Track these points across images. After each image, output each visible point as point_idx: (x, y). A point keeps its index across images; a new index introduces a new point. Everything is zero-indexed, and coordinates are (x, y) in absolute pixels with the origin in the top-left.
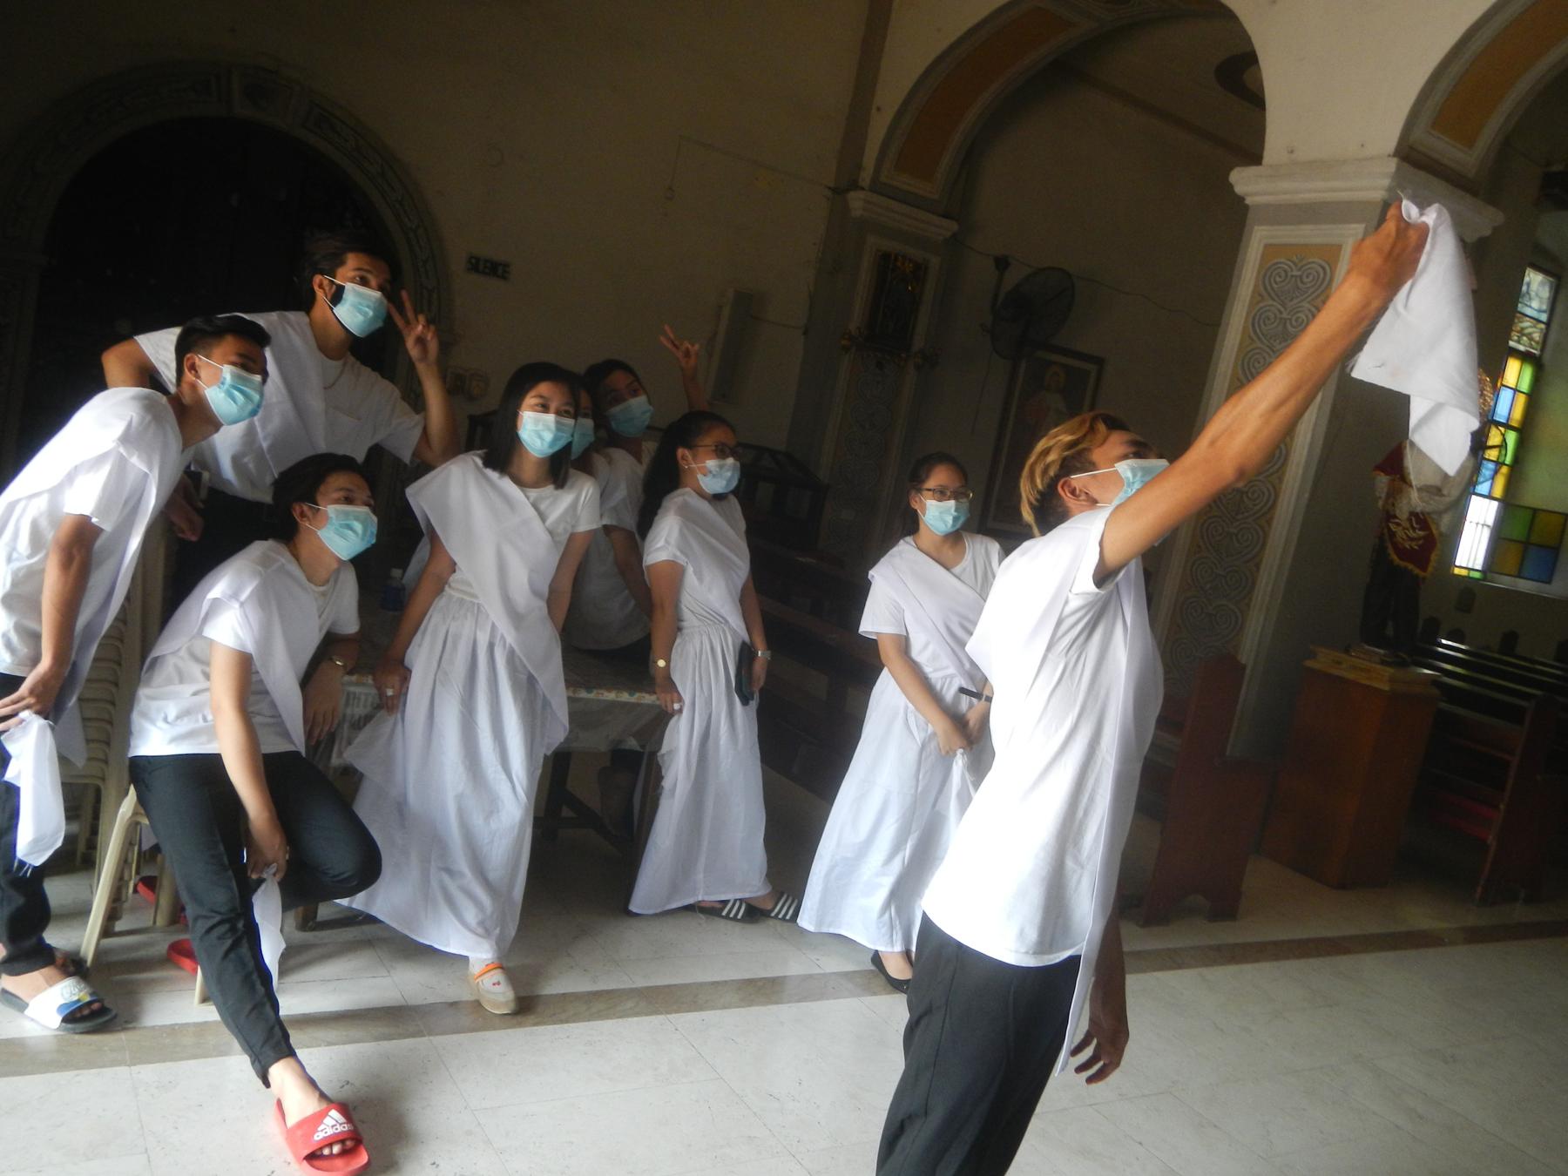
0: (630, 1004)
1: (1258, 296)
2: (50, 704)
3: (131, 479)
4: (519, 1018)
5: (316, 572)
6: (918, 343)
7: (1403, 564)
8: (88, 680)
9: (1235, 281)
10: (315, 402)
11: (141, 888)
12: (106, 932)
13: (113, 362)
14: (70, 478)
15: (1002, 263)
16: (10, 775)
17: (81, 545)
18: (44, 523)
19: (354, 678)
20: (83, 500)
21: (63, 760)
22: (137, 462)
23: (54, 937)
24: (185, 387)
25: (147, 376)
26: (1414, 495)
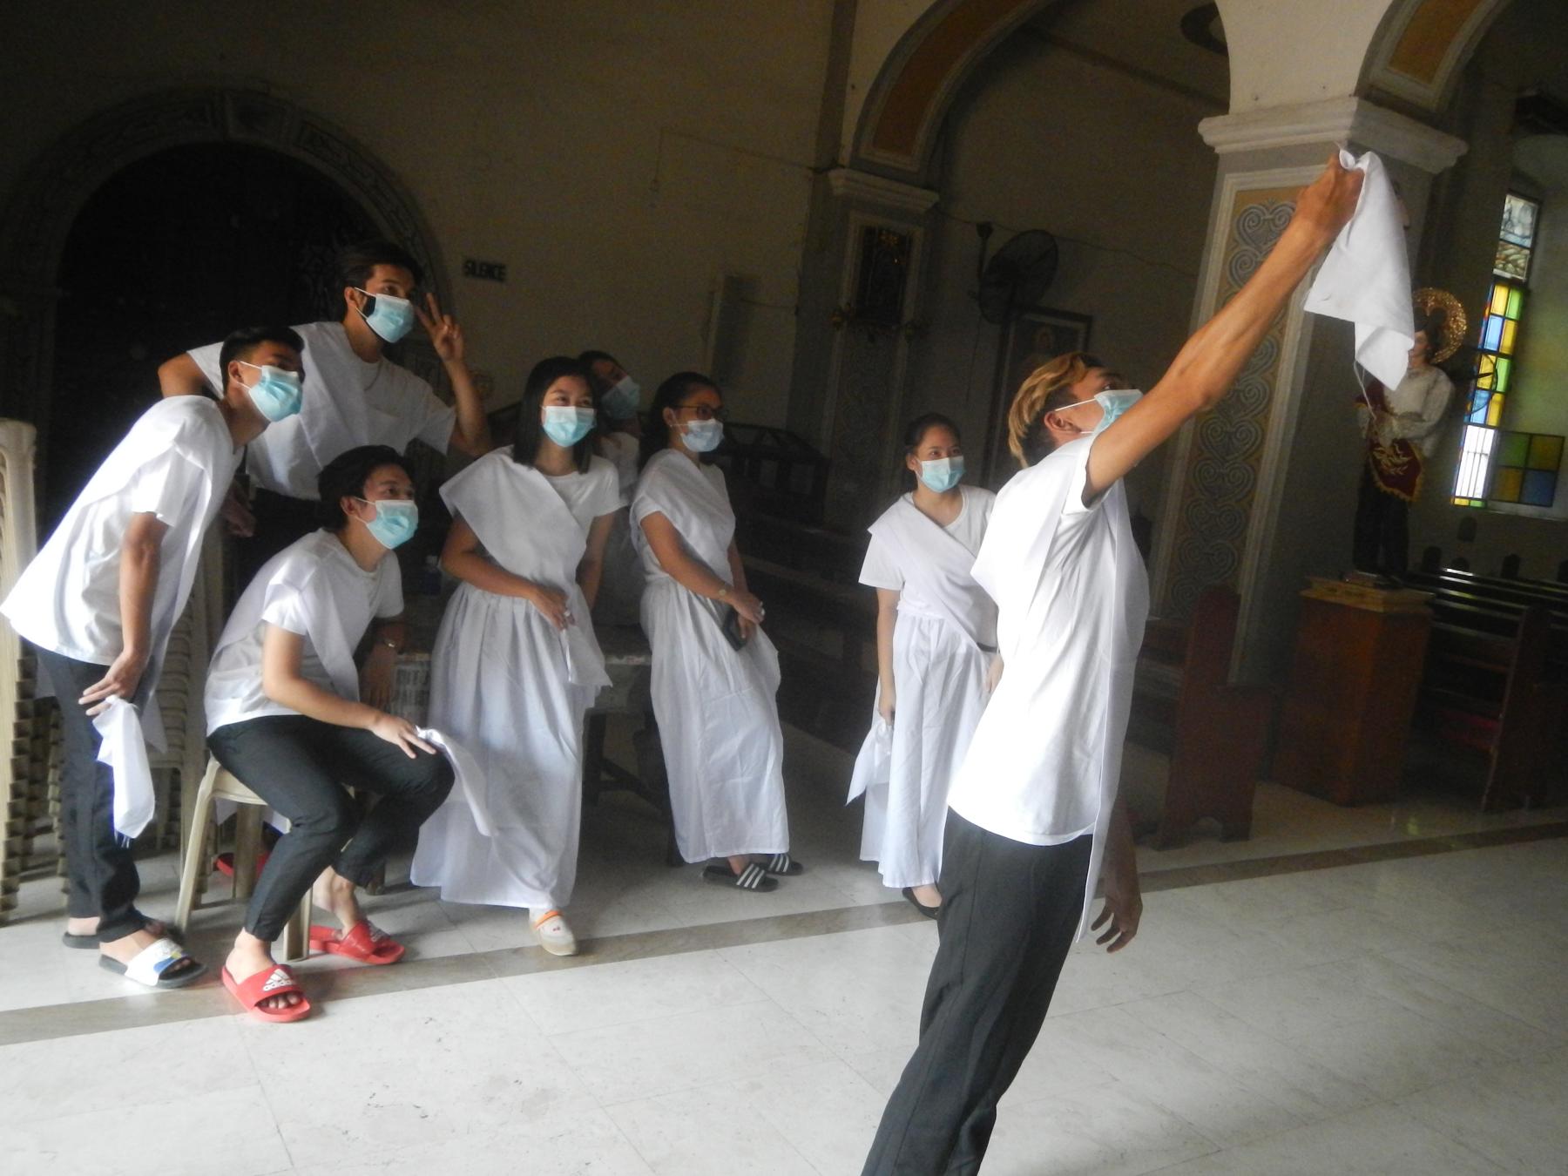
0: (680, 942)
1: (1232, 242)
2: (134, 689)
3: (189, 478)
4: (579, 958)
6: (908, 314)
7: (1389, 490)
9: (1209, 230)
11: (221, 865)
12: (196, 904)
14: (135, 480)
15: (985, 230)
16: (102, 756)
17: (150, 541)
18: (115, 524)
19: (403, 657)
20: (149, 499)
22: (193, 460)
23: (147, 909)
24: (231, 393)
26: (1395, 423)
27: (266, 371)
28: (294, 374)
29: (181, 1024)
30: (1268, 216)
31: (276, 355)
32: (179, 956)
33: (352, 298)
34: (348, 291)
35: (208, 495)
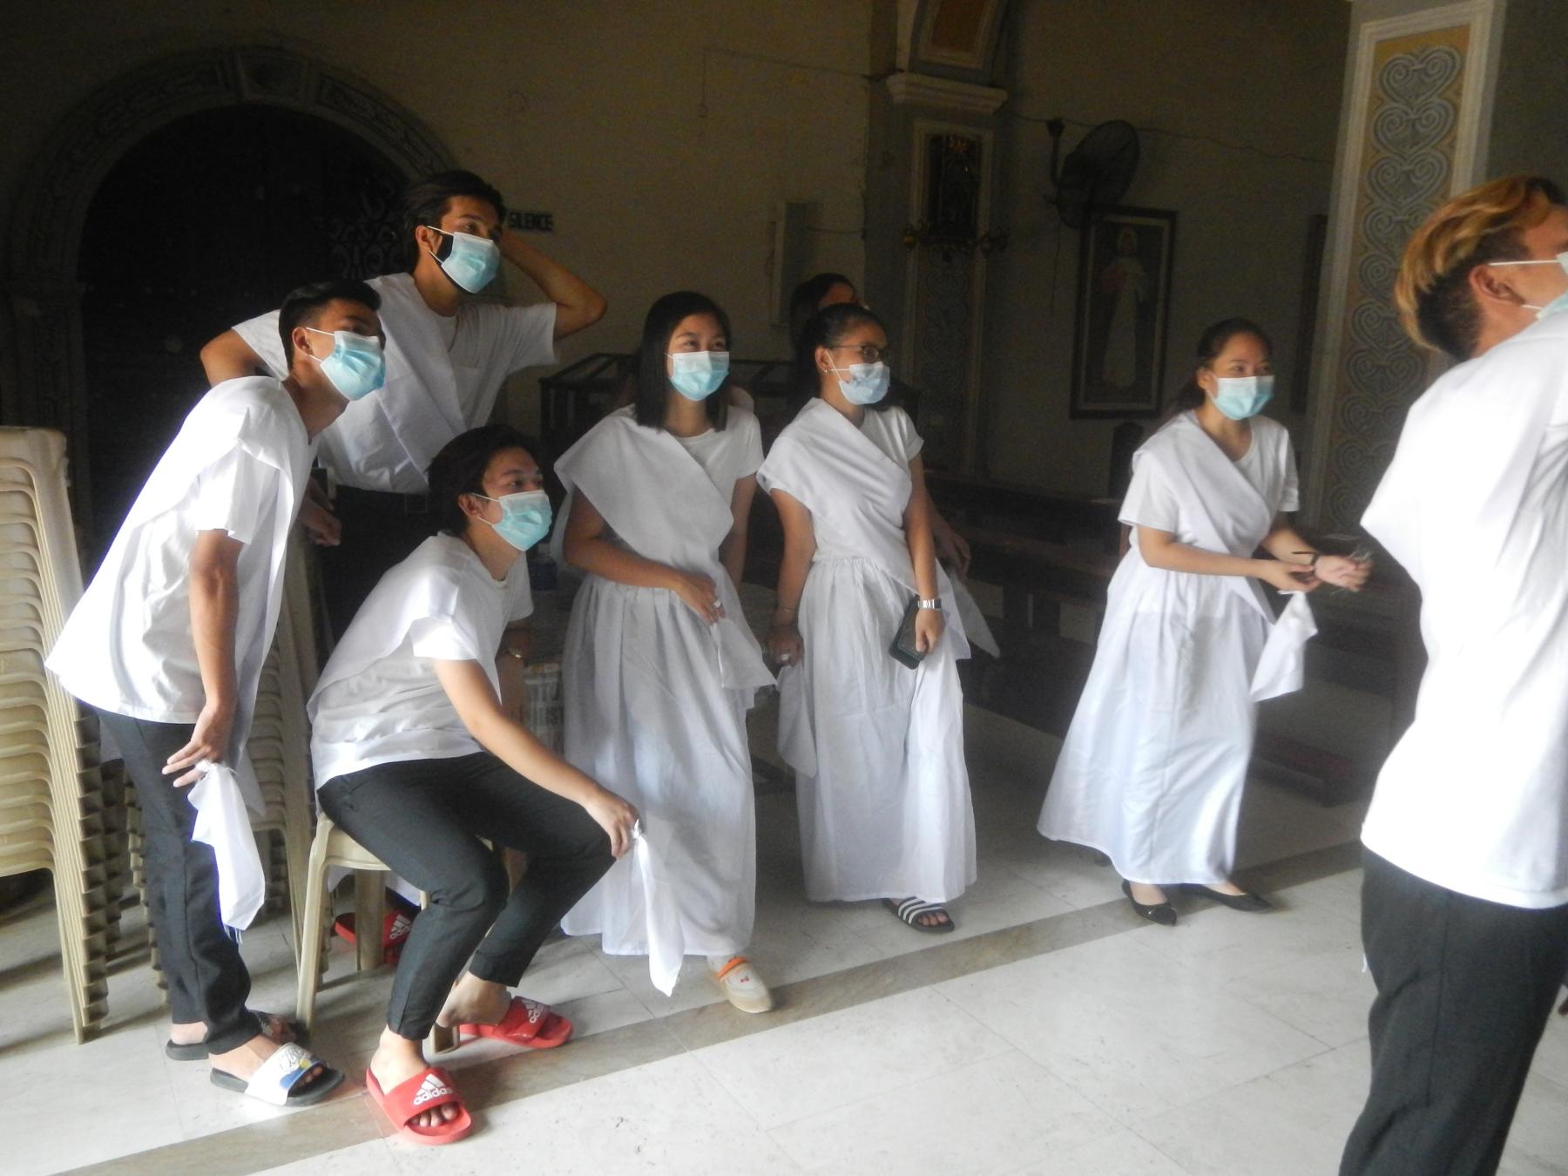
0: (889, 980)
2: (222, 747)
3: (261, 481)
4: (778, 1014)
5: (492, 558)
6: (983, 227)
8: (257, 717)
9: (1346, 90)
10: (442, 371)
11: (339, 928)
12: (320, 986)
13: (213, 357)
14: (195, 490)
15: (1055, 127)
17: (223, 565)
18: (175, 547)
19: (529, 670)
20: (215, 512)
21: (249, 809)
22: (265, 459)
24: (299, 369)
25: (253, 366)
27: (340, 338)
28: (374, 340)
29: (322, 1158)
30: (1417, 67)
31: (350, 317)
32: (309, 1065)
33: (424, 238)
34: (420, 230)
35: (289, 500)
